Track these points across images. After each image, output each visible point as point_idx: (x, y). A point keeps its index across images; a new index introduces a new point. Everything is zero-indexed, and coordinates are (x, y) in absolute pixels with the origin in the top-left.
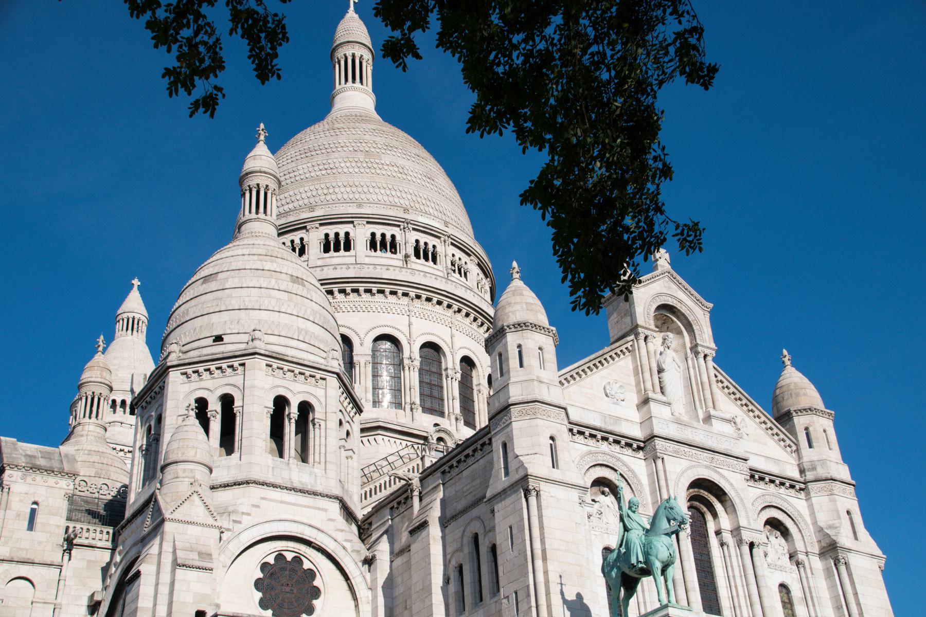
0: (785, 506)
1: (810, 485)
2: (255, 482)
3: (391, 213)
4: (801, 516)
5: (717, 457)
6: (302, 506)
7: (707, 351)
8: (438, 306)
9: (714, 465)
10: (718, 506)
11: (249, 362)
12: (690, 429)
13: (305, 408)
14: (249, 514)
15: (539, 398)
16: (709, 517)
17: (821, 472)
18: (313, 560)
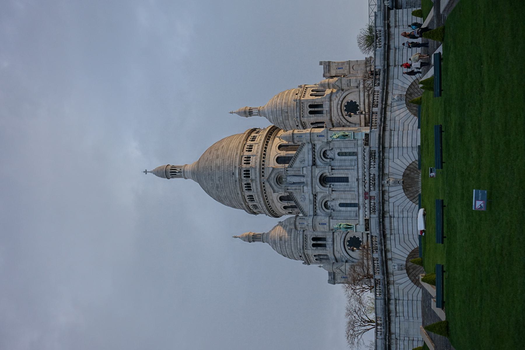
0: (319, 151)
2: (334, 253)
3: (238, 186)
4: (320, 147)
6: (337, 242)
7: (286, 171)
8: (264, 172)
10: (324, 175)
11: (306, 253)
12: (308, 183)
13: (314, 239)
14: (341, 254)
15: (312, 227)
16: (327, 176)
17: (309, 141)
18: (348, 238)
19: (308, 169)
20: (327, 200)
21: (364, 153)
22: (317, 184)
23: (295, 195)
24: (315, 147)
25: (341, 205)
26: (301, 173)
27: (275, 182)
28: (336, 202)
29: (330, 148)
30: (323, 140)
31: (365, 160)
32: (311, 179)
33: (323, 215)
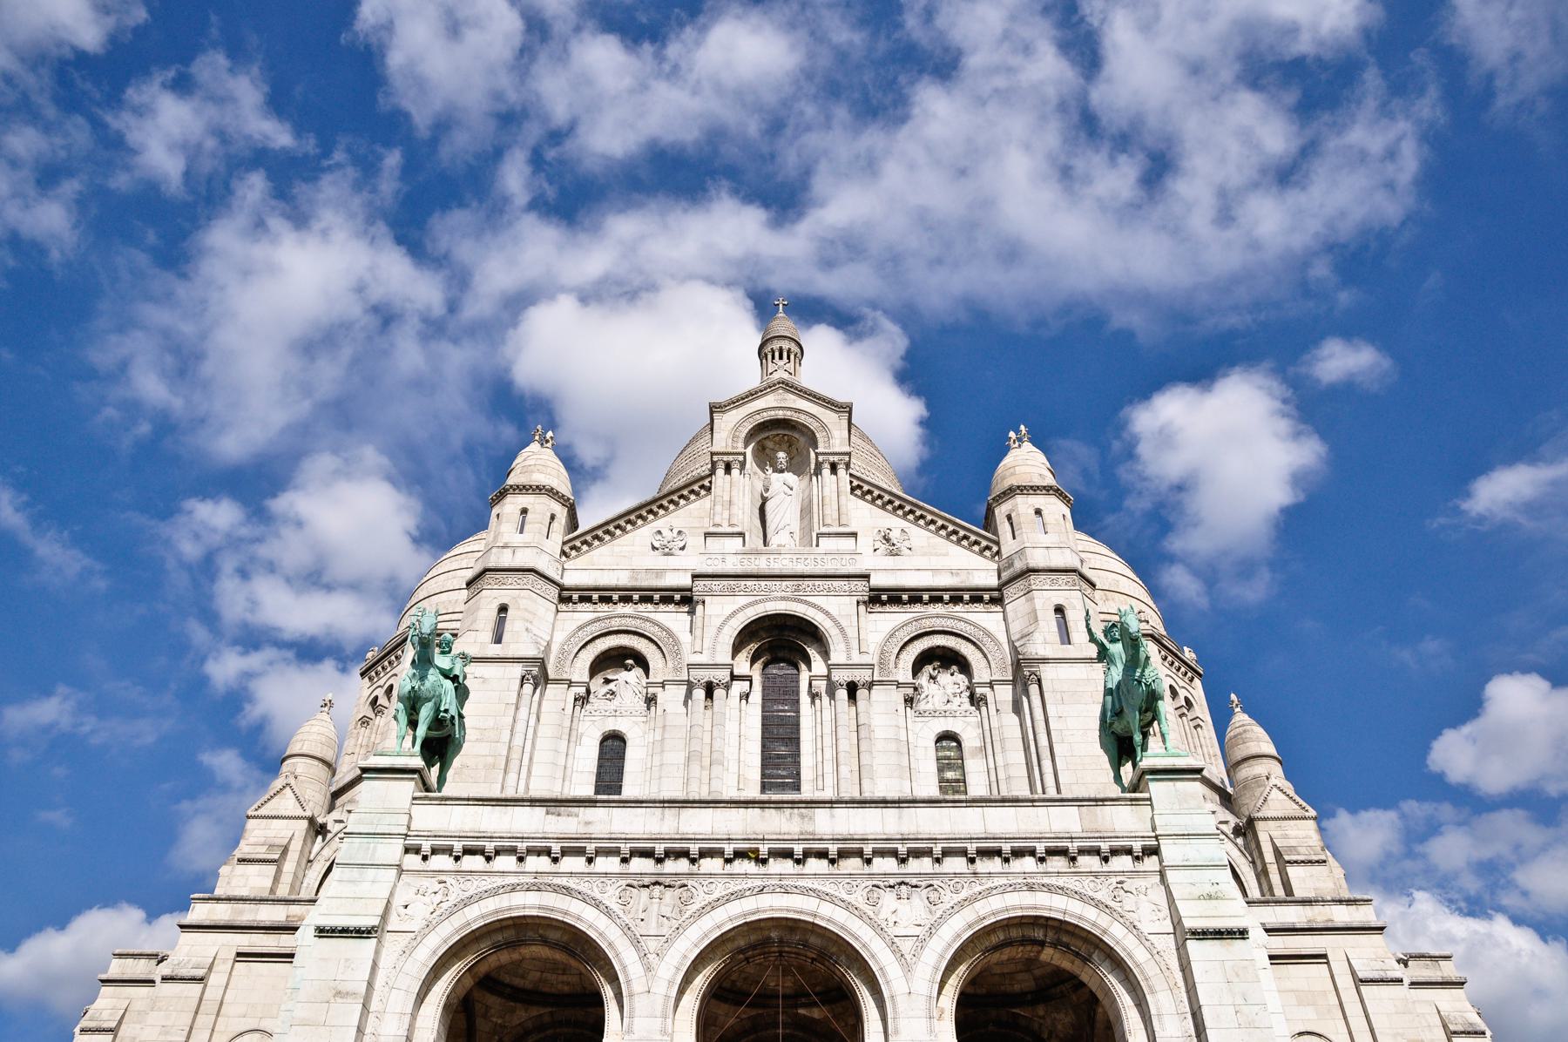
1: (1009, 592)
5: (806, 583)
7: (832, 458)
9: (801, 593)
12: (764, 557)
15: (491, 565)
16: (803, 667)
17: (1019, 566)
19: (848, 557)
20: (651, 666)
21: (1040, 848)
22: (756, 603)
23: (691, 506)
24: (979, 607)
25: (613, 745)
26: (824, 530)
27: (773, 413)
28: (634, 719)
29: (982, 684)
30: (1038, 637)
31: (972, 861)
32: (785, 572)
33: (559, 637)
